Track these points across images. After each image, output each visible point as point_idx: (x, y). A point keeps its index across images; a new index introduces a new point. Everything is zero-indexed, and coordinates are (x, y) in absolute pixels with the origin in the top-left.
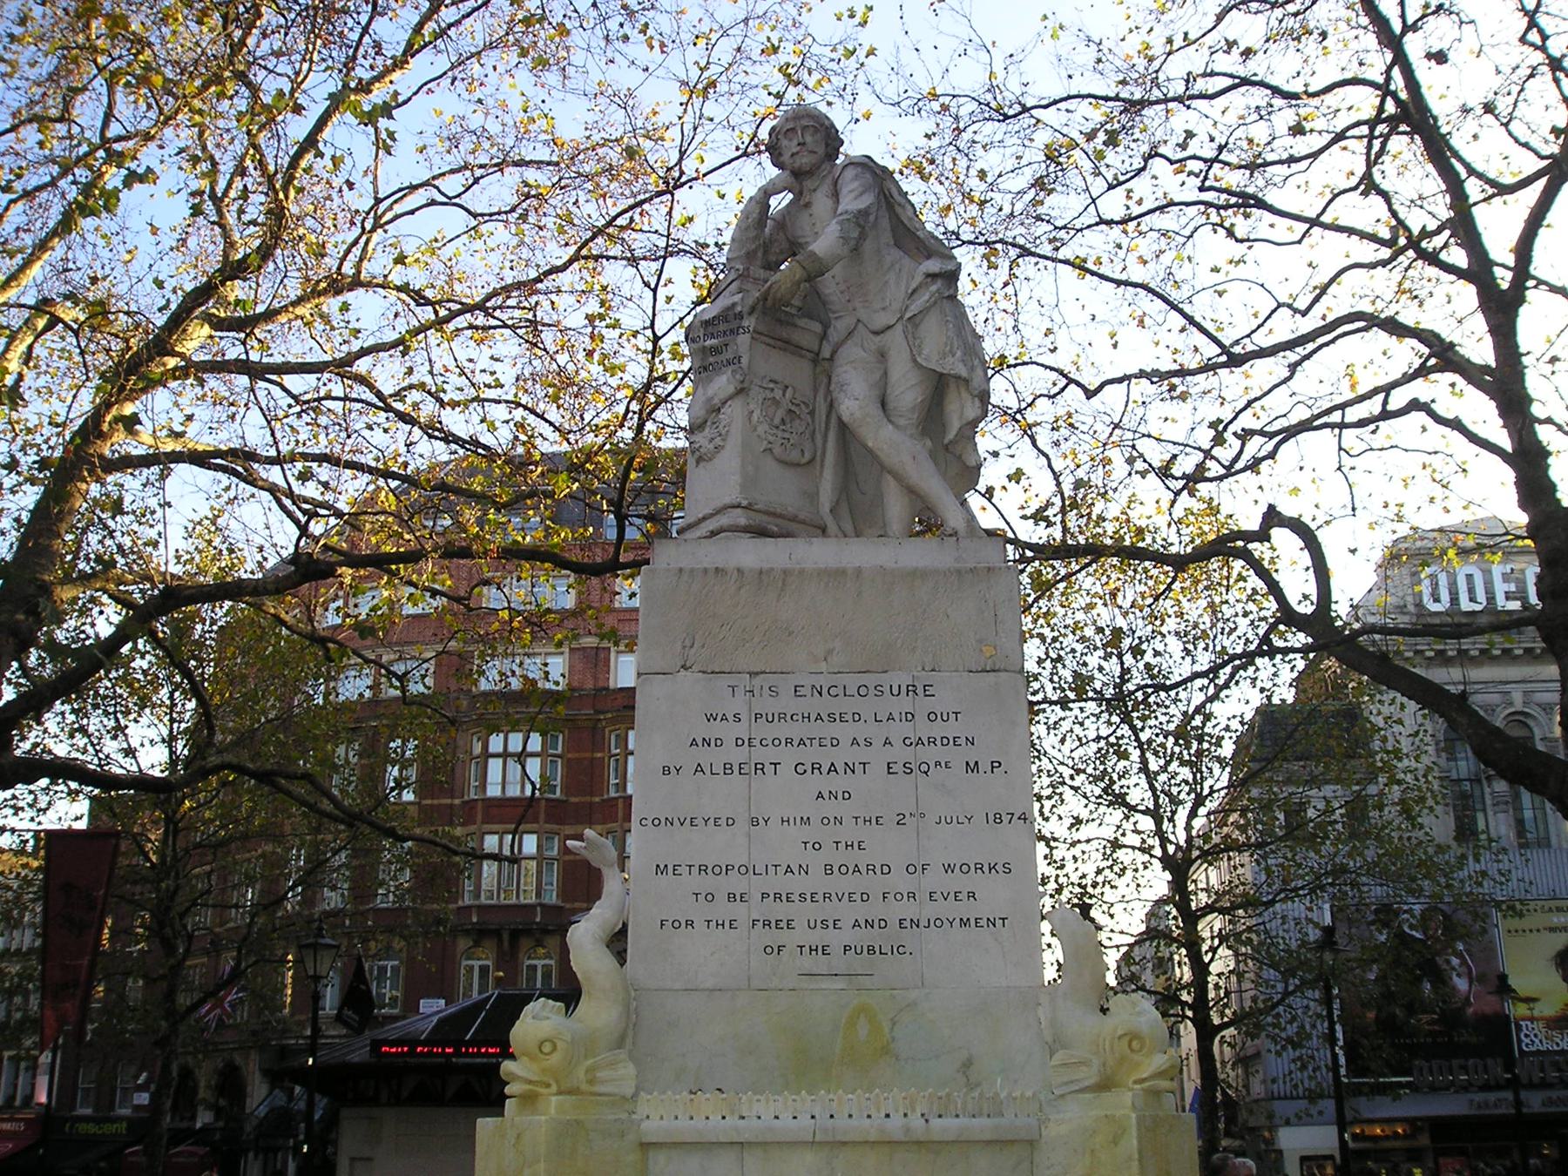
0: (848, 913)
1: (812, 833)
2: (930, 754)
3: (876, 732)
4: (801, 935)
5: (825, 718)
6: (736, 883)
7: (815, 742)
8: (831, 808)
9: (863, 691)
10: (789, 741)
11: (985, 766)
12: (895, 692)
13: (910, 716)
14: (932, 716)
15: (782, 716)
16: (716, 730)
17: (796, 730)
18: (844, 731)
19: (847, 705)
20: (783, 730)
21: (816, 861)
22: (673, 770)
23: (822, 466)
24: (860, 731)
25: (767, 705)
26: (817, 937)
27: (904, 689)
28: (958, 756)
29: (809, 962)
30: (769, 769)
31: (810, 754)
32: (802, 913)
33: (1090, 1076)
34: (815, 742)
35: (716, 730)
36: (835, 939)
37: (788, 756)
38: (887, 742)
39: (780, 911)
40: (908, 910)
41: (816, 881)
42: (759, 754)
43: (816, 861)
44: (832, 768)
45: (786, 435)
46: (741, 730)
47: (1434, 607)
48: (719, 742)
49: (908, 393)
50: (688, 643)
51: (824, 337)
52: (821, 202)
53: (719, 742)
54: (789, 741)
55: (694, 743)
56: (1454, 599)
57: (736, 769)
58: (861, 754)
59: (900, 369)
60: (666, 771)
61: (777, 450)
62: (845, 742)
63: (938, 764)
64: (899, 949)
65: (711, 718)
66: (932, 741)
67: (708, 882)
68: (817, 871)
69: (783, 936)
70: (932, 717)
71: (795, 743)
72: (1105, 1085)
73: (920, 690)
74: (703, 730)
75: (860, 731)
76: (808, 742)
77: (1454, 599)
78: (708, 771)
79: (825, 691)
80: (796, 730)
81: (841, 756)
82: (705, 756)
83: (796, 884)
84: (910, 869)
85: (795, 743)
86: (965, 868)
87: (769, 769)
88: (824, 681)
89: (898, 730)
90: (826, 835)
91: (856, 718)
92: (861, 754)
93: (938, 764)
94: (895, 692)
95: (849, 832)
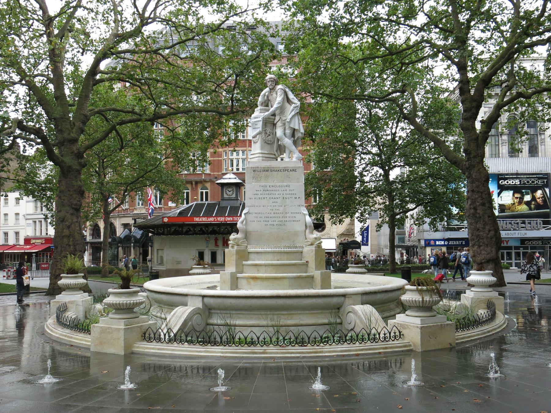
0: (277, 220)
1: (272, 208)
3: (282, 193)
4: (270, 223)
6: (260, 215)
8: (275, 204)
14: (290, 190)
16: (258, 192)
17: (270, 192)
18: (277, 193)
19: (277, 189)
20: (267, 192)
21: (272, 212)
24: (279, 192)
25: (266, 189)
26: (272, 223)
28: (294, 196)
29: (271, 226)
31: (271, 196)
32: (270, 219)
33: (310, 243)
36: (275, 223)
37: (268, 196)
39: (267, 219)
40: (285, 219)
41: (273, 215)
43: (272, 212)
46: (261, 192)
49: (288, 132)
51: (274, 119)
52: (274, 95)
58: (279, 196)
59: (287, 127)
67: (256, 215)
68: (272, 213)
69: (266, 223)
72: (312, 244)
74: (256, 192)
75: (279, 192)
82: (256, 196)
83: (270, 215)
84: (286, 213)
86: (294, 213)
90: (274, 208)
91: (278, 190)
95: (277, 208)
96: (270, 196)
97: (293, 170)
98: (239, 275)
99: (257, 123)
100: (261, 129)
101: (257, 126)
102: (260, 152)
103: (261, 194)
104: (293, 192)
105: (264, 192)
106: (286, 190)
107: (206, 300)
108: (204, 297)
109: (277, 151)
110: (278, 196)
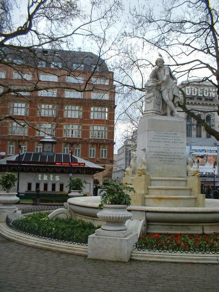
2: (176, 141)
3: (171, 138)
17: (163, 138)
37: (163, 140)
39: (162, 157)
41: (165, 154)
47: (188, 94)
52: (162, 72)
56: (191, 93)
58: (170, 141)
64: (173, 161)
77: (191, 93)
80: (163, 138)
81: (168, 141)
83: (163, 154)
89: (173, 138)
92: (170, 141)
98: (147, 196)
104: (179, 138)
107: (148, 214)
108: (147, 211)
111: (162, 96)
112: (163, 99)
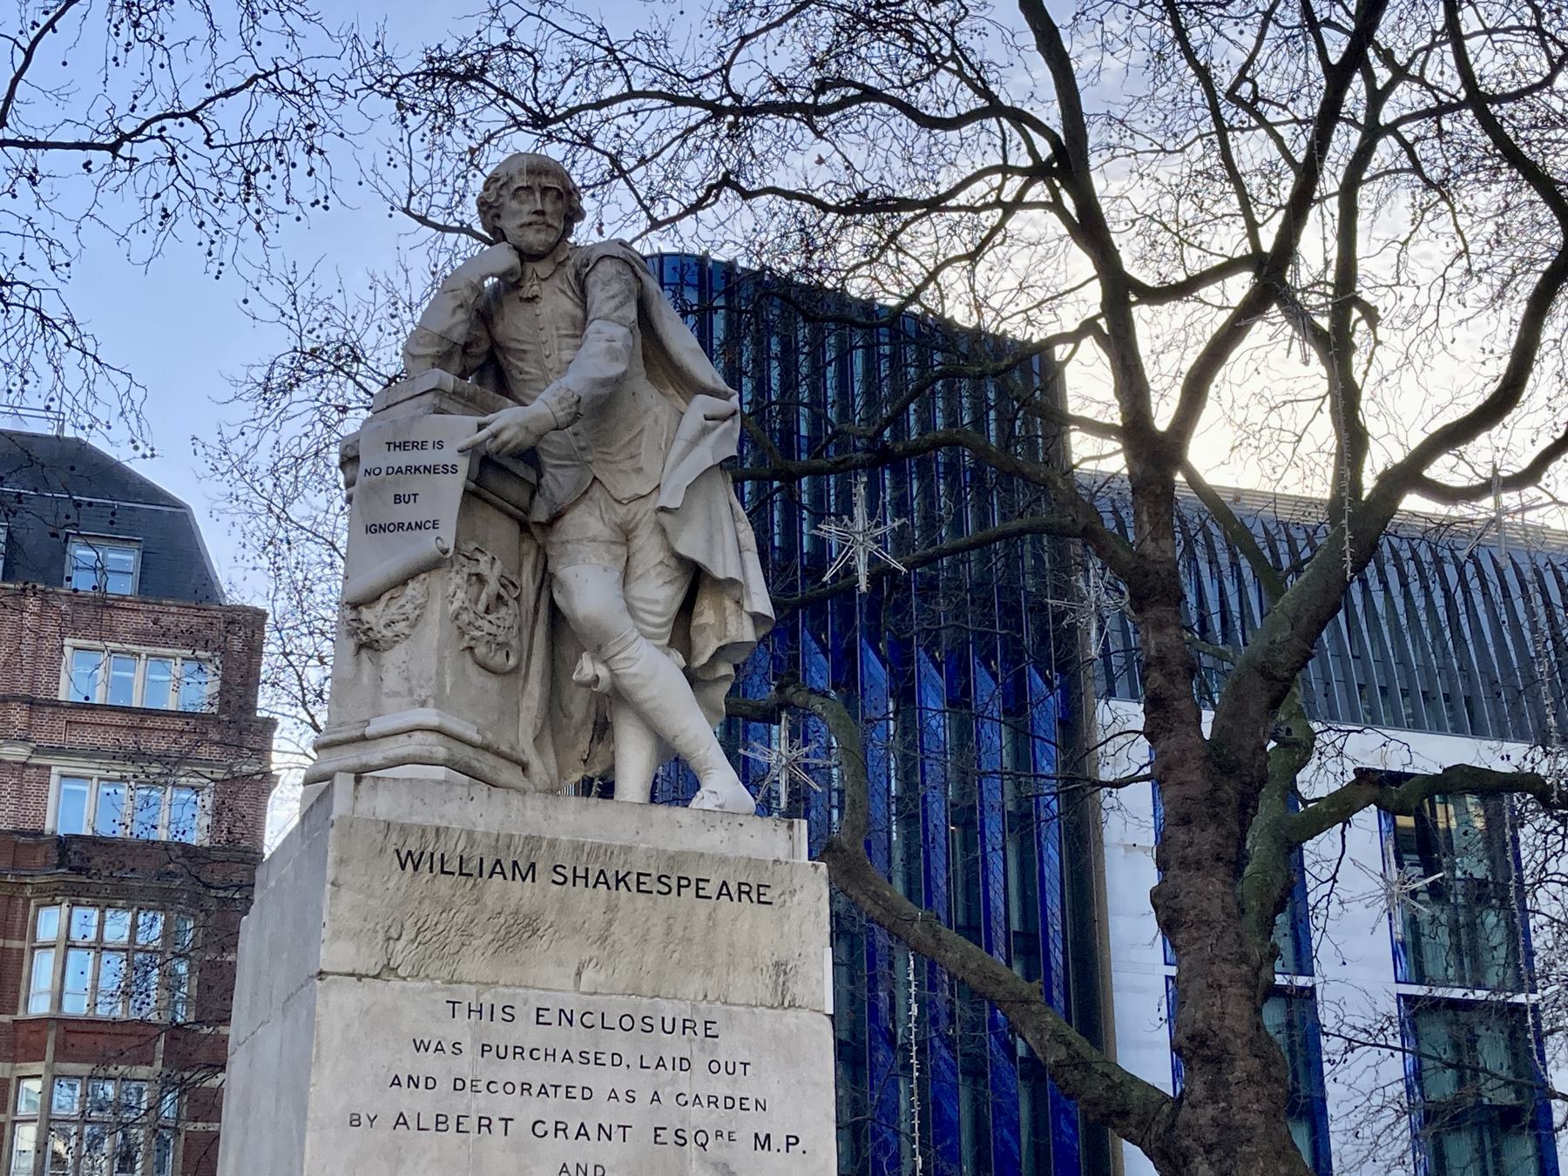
3: (643, 1084)
5: (576, 1057)
7: (562, 1091)
9: (627, 1023)
10: (526, 1088)
11: (778, 1141)
12: (668, 1028)
13: (684, 1064)
14: (714, 1067)
15: (518, 1051)
16: (428, 1064)
17: (537, 1073)
18: (602, 1080)
20: (514, 1070)
22: (364, 1120)
23: (527, 674)
25: (501, 1034)
27: (679, 1024)
28: (747, 1125)
30: (498, 1126)
31: (550, 1109)
34: (562, 1091)
35: (428, 1064)
37: (528, 1109)
38: (656, 1097)
42: (481, 1103)
44: (582, 1131)
45: (493, 630)
48: (431, 1083)
49: (659, 593)
50: (394, 933)
53: (431, 1083)
54: (526, 1088)
55: (396, 1082)
57: (452, 1124)
60: (355, 1121)
61: (481, 650)
62: (601, 1093)
63: (719, 1134)
65: (419, 1046)
66: (713, 1101)
70: (714, 1067)
71: (535, 1090)
73: (700, 1029)
74: (410, 1063)
75: (620, 1079)
76: (551, 1091)
78: (412, 1124)
79: (577, 1017)
80: (537, 1073)
85: (535, 1090)
87: (498, 1126)
88: (572, 1003)
91: (617, 1059)
93: (719, 1134)
94: (668, 1028)
96: (535, 1107)
97: (743, 891)
99: (416, 483)
100: (448, 535)
101: (405, 513)
102: (430, 716)
103: (458, 1085)
105: (490, 1069)
106: (684, 1064)
109: (537, 739)
110: (609, 1114)
111: (546, 580)
112: (554, 609)
